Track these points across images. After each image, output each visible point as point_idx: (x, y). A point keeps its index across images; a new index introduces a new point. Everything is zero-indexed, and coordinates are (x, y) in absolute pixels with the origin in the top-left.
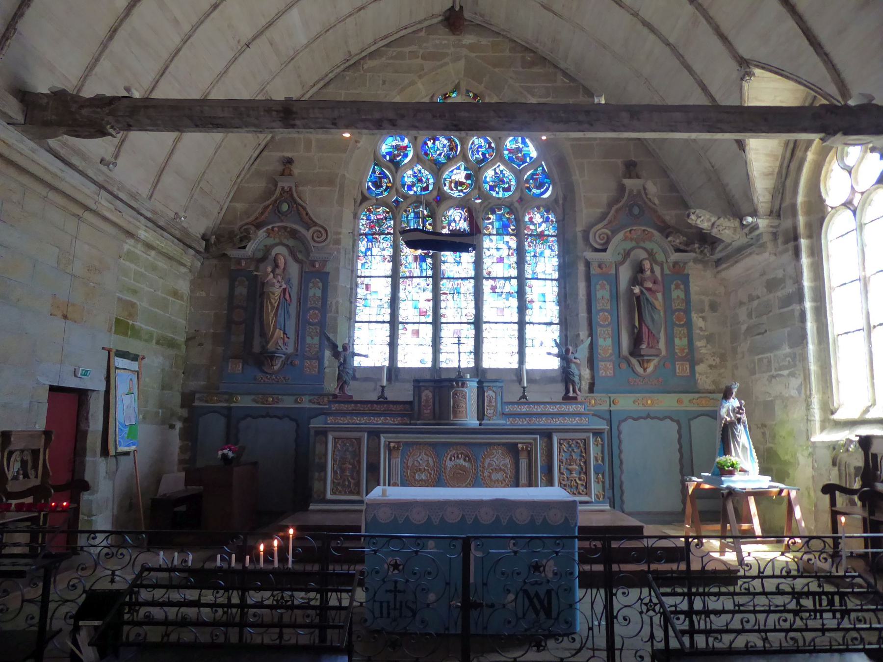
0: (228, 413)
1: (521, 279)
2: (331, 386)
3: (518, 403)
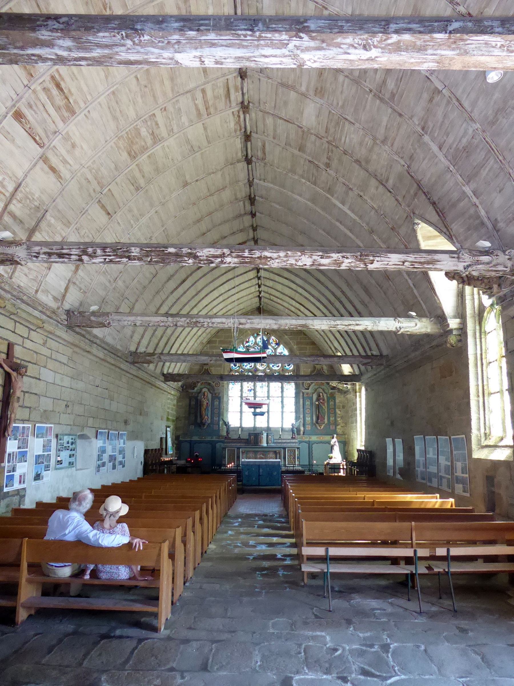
0: (190, 442)
1: (282, 397)
2: (225, 434)
3: (279, 439)
